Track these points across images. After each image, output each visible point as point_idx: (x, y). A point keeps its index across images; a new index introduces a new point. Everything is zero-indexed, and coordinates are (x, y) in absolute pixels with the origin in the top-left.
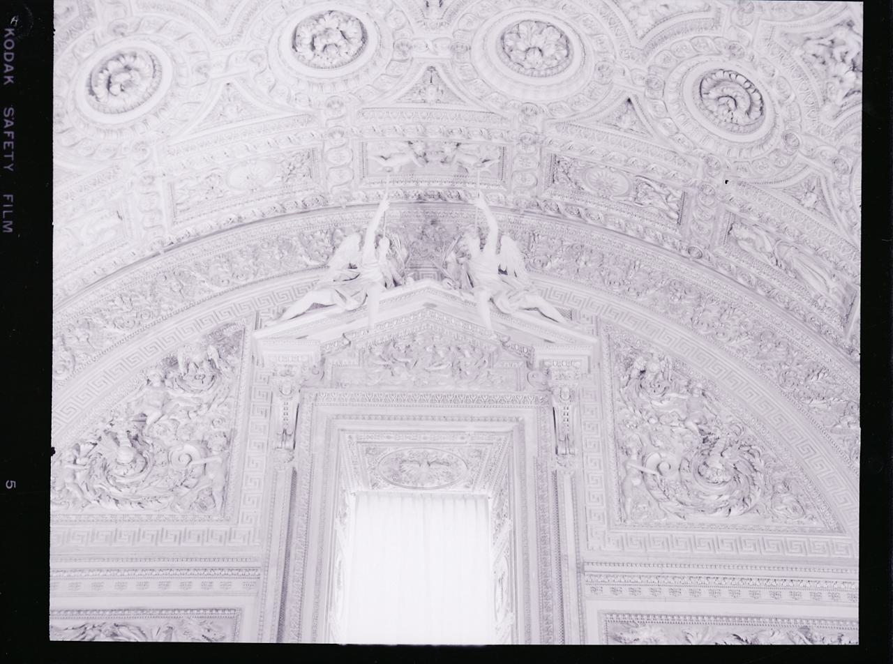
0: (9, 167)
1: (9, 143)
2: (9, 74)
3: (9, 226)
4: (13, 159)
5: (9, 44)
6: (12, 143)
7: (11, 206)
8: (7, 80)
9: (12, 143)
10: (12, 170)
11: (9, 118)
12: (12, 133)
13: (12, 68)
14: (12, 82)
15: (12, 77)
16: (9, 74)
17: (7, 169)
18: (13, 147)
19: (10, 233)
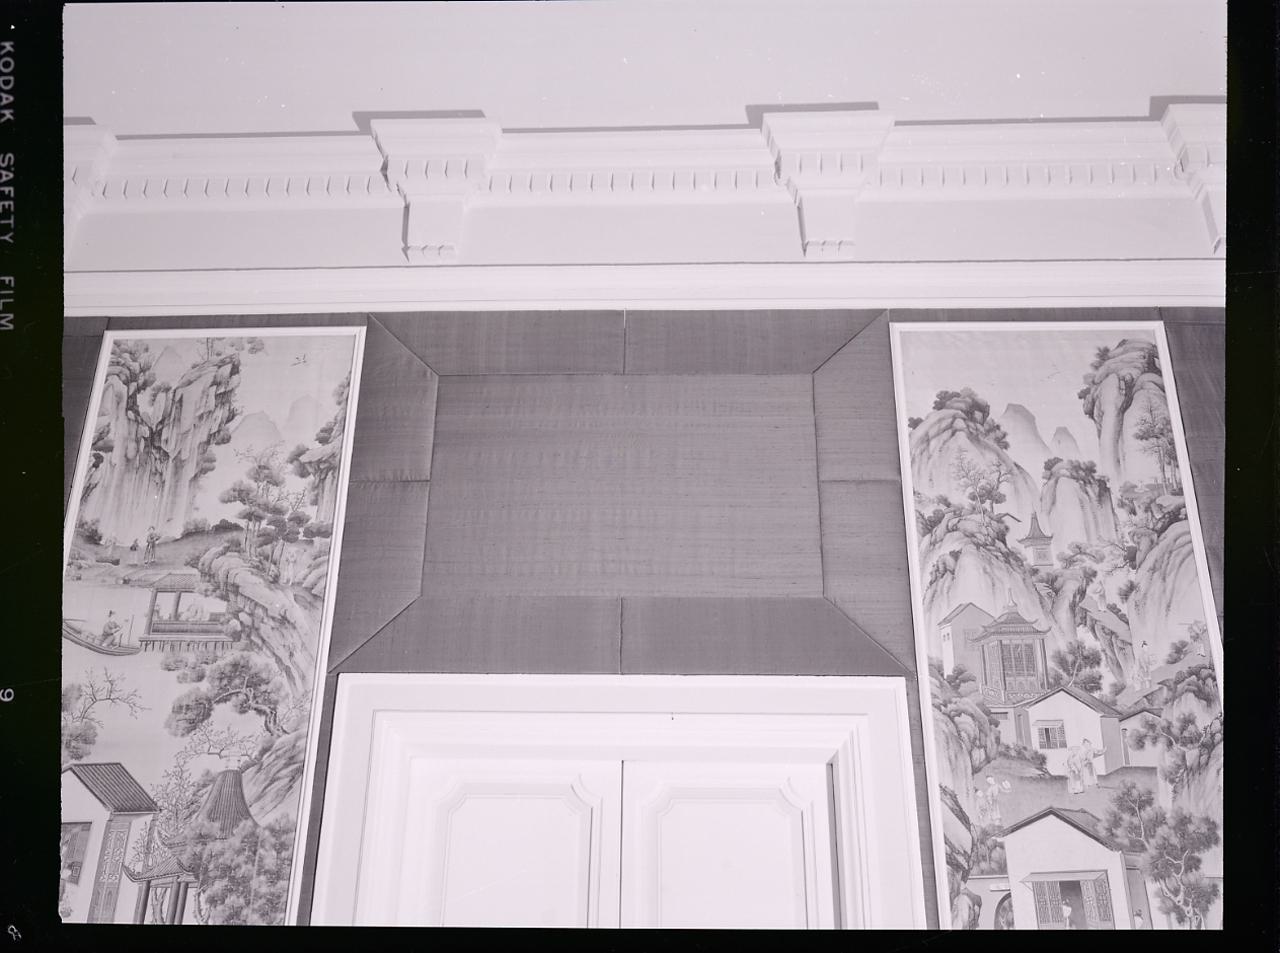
0: (7, 238)
1: (7, 203)
2: (6, 107)
3: (8, 322)
4: (12, 226)
5: (6, 65)
6: (12, 203)
7: (12, 292)
8: (4, 115)
9: (12, 203)
10: (11, 241)
11: (7, 169)
12: (12, 189)
13: (11, 98)
14: (12, 118)
15: (11, 111)
16: (6, 107)
17: (5, 241)
18: (12, 209)
19: (10, 331)
